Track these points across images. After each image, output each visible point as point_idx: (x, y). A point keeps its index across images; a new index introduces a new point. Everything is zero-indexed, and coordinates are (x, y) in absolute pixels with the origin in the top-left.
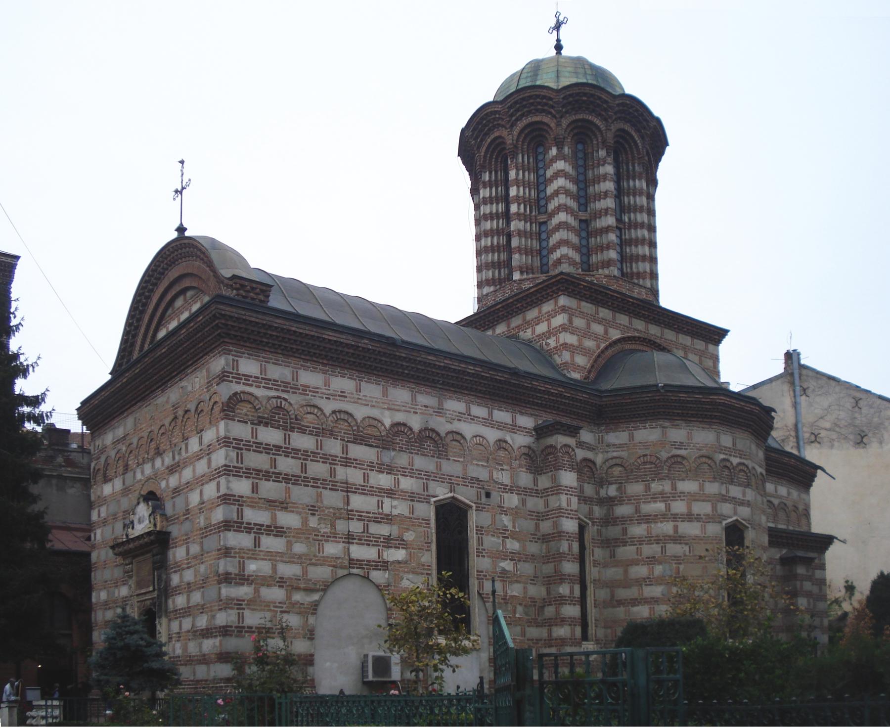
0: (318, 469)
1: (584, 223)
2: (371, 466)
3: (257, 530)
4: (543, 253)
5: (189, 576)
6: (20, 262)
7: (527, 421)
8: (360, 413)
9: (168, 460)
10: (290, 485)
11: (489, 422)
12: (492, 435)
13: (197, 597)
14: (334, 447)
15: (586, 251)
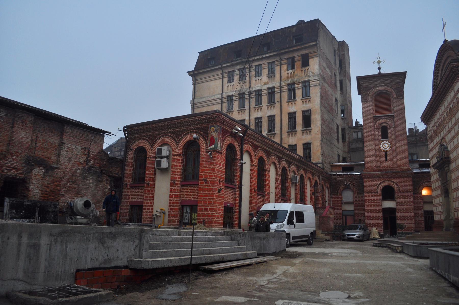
9: (447, 129)
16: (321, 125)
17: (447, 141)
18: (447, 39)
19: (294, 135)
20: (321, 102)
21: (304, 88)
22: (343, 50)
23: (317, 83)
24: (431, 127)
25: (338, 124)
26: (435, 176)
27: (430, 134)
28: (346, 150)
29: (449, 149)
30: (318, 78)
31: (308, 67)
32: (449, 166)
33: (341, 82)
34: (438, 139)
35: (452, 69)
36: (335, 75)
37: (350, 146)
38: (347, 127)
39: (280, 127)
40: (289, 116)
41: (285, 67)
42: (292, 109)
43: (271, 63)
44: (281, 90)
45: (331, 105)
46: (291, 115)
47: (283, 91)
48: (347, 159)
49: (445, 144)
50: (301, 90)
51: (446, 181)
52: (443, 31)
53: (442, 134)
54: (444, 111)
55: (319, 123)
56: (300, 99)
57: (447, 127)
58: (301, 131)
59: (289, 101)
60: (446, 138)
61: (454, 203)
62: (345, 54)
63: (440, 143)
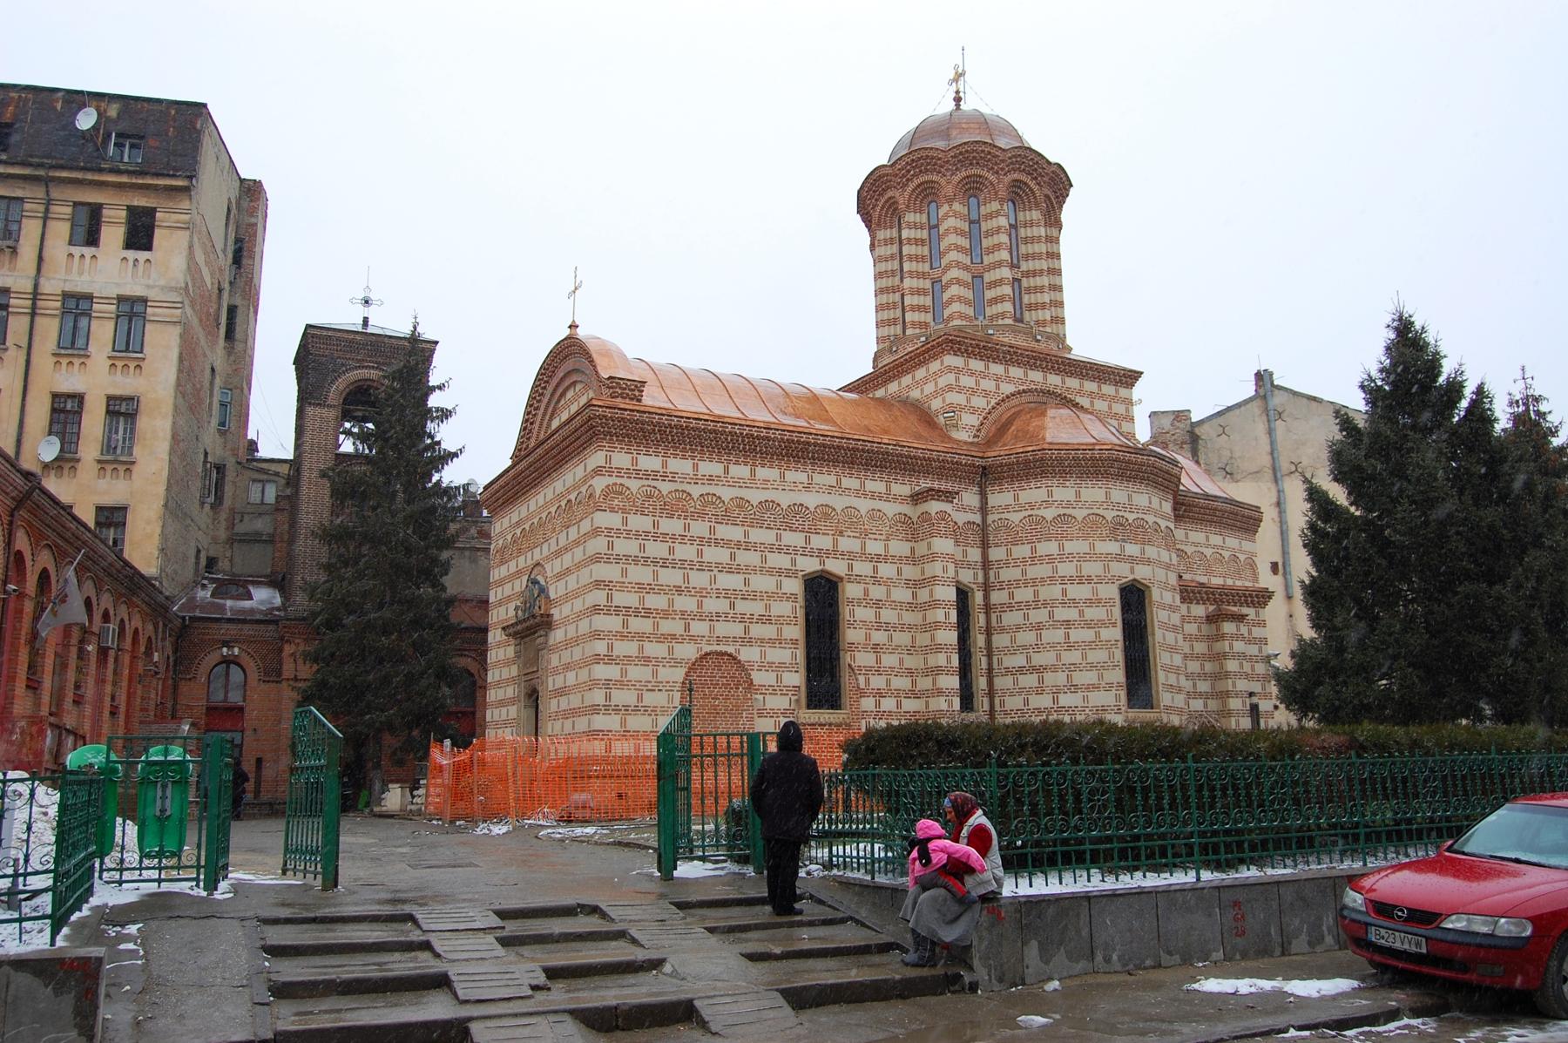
0: (686, 552)
1: (978, 277)
2: (738, 545)
3: (627, 612)
4: (936, 308)
5: (566, 656)
6: (438, 347)
7: (902, 489)
8: (727, 494)
9: (554, 548)
10: (658, 568)
11: (861, 493)
12: (864, 505)
13: (571, 678)
14: (699, 528)
15: (979, 304)
16: (170, 454)
17: (549, 574)
18: (577, 323)
19: (66, 471)
20: (178, 377)
21: (124, 322)
22: (252, 212)
23: (172, 316)
24: (504, 526)
25: (208, 450)
26: (501, 651)
27: (501, 542)
28: (222, 534)
29: (552, 596)
30: (179, 300)
31: (143, 255)
32: (546, 635)
33: (232, 310)
34: (523, 562)
35: (590, 419)
36: (220, 290)
37: (233, 524)
38: (233, 460)
39: (15, 434)
40: (53, 403)
41: (60, 230)
42: (69, 381)
43: (6, 201)
44: (34, 306)
45: (198, 386)
46: (62, 400)
47: (42, 311)
48: (220, 564)
49: (540, 578)
50: (111, 325)
51: (535, 669)
52: (572, 298)
53: (537, 555)
54: (552, 502)
55: (163, 447)
56: (105, 355)
57: (553, 541)
58: (95, 464)
59: (63, 352)
60: (548, 567)
61: (550, 724)
62: (256, 224)
63: (528, 573)
